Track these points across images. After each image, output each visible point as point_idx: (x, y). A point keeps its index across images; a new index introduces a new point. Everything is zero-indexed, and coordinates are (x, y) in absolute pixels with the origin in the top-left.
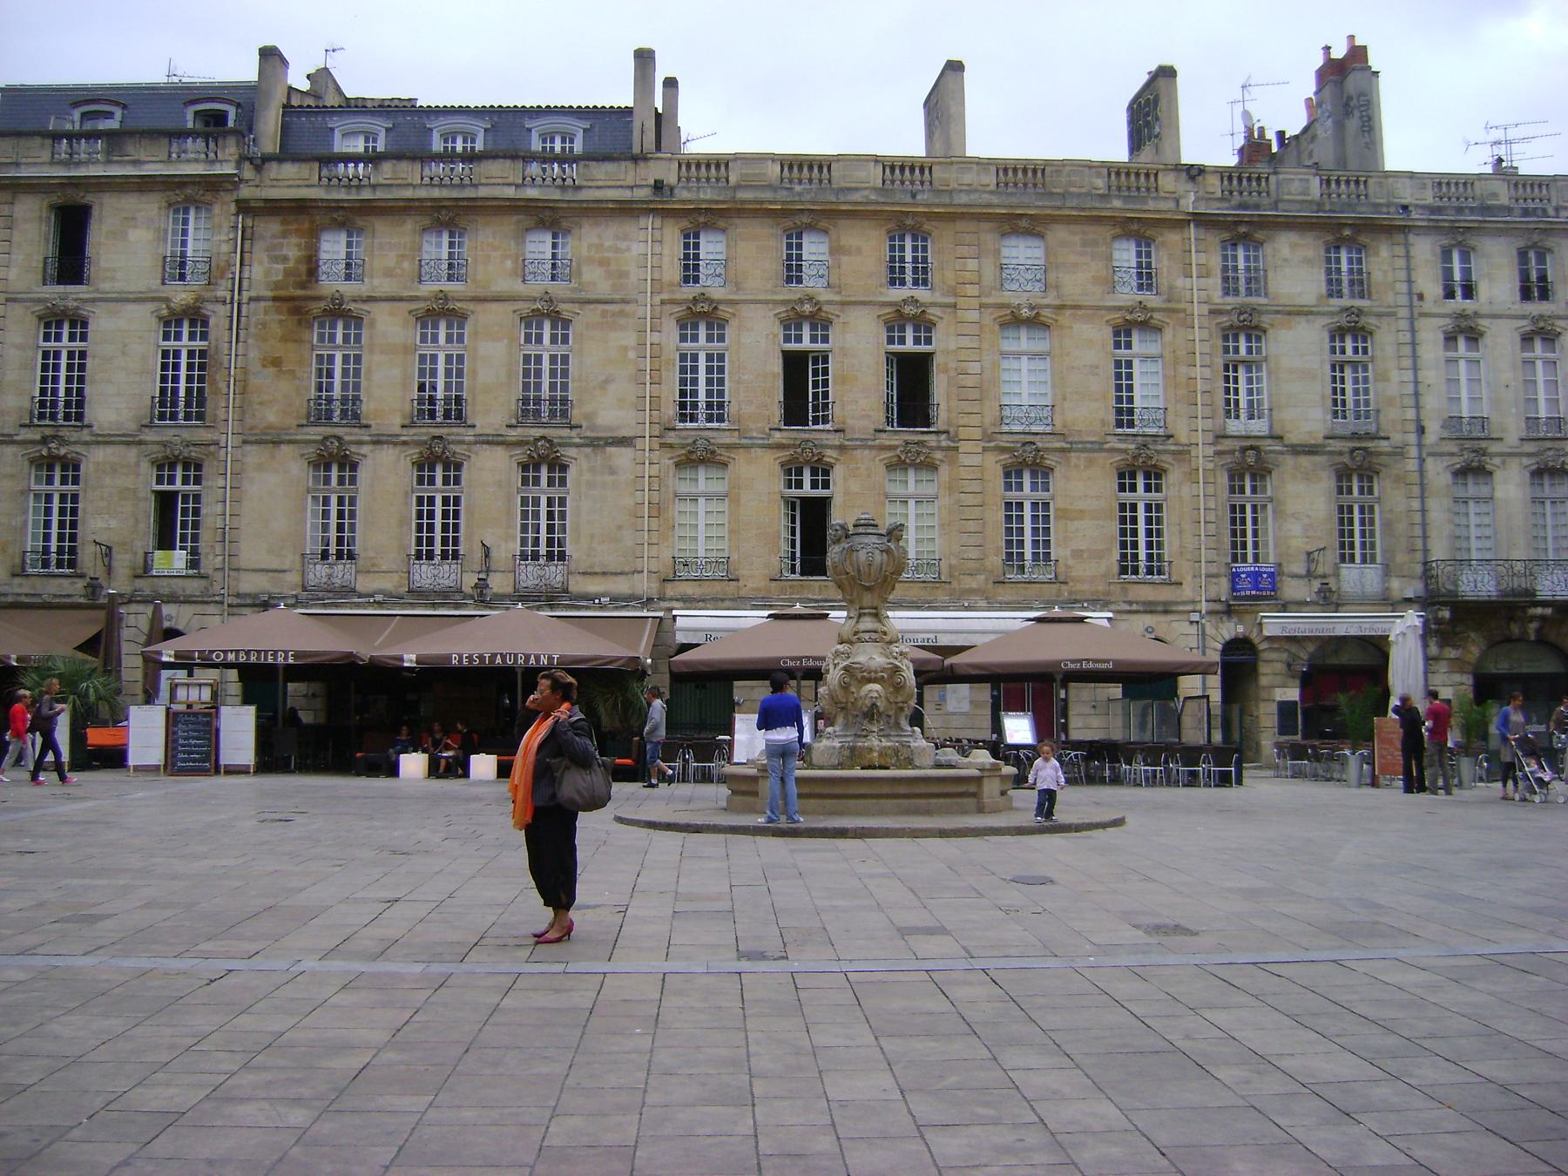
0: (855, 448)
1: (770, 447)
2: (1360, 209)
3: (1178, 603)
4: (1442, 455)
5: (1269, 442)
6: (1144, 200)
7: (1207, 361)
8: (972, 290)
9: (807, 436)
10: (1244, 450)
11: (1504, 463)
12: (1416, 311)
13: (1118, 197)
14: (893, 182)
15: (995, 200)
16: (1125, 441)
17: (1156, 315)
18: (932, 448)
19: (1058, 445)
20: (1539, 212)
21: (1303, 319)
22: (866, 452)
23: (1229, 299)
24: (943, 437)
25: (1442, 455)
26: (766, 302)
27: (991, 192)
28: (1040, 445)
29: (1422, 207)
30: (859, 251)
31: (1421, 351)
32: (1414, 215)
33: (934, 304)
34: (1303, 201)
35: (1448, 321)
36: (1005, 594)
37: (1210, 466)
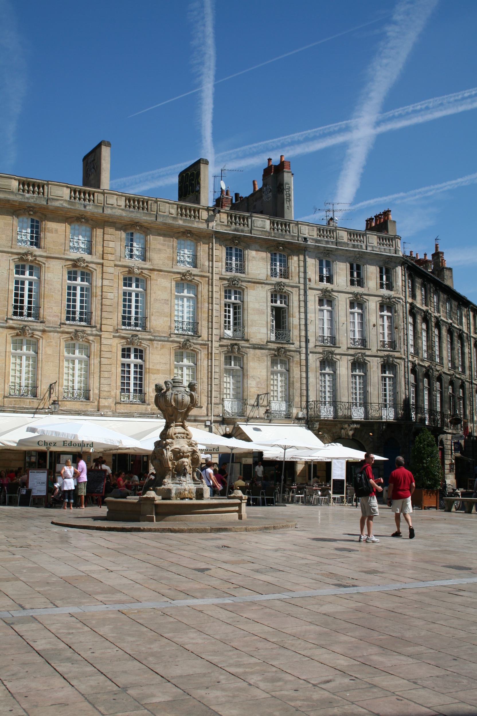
0: (50, 332)
1: (7, 328)
2: (286, 237)
3: (201, 416)
4: (316, 353)
5: (243, 342)
6: (193, 222)
7: (218, 302)
8: (110, 257)
9: (26, 323)
10: (232, 345)
11: (341, 358)
12: (308, 287)
13: (181, 219)
14: (75, 198)
15: (124, 214)
16: (179, 337)
17: (196, 278)
18: (88, 334)
19: (149, 337)
20: (359, 247)
21: (260, 286)
22: (56, 334)
23: (229, 273)
24: (94, 329)
25: (316, 353)
26: (8, 252)
27: (123, 210)
28: (140, 336)
29: (312, 239)
30: (56, 231)
31: (309, 304)
32: (309, 243)
33: (92, 263)
34: (263, 231)
35: (320, 292)
36: (121, 409)
37: (217, 352)
